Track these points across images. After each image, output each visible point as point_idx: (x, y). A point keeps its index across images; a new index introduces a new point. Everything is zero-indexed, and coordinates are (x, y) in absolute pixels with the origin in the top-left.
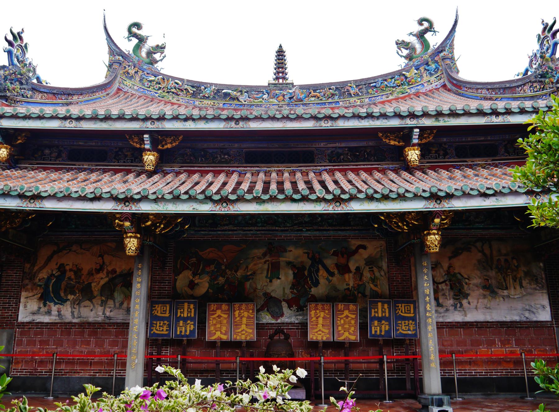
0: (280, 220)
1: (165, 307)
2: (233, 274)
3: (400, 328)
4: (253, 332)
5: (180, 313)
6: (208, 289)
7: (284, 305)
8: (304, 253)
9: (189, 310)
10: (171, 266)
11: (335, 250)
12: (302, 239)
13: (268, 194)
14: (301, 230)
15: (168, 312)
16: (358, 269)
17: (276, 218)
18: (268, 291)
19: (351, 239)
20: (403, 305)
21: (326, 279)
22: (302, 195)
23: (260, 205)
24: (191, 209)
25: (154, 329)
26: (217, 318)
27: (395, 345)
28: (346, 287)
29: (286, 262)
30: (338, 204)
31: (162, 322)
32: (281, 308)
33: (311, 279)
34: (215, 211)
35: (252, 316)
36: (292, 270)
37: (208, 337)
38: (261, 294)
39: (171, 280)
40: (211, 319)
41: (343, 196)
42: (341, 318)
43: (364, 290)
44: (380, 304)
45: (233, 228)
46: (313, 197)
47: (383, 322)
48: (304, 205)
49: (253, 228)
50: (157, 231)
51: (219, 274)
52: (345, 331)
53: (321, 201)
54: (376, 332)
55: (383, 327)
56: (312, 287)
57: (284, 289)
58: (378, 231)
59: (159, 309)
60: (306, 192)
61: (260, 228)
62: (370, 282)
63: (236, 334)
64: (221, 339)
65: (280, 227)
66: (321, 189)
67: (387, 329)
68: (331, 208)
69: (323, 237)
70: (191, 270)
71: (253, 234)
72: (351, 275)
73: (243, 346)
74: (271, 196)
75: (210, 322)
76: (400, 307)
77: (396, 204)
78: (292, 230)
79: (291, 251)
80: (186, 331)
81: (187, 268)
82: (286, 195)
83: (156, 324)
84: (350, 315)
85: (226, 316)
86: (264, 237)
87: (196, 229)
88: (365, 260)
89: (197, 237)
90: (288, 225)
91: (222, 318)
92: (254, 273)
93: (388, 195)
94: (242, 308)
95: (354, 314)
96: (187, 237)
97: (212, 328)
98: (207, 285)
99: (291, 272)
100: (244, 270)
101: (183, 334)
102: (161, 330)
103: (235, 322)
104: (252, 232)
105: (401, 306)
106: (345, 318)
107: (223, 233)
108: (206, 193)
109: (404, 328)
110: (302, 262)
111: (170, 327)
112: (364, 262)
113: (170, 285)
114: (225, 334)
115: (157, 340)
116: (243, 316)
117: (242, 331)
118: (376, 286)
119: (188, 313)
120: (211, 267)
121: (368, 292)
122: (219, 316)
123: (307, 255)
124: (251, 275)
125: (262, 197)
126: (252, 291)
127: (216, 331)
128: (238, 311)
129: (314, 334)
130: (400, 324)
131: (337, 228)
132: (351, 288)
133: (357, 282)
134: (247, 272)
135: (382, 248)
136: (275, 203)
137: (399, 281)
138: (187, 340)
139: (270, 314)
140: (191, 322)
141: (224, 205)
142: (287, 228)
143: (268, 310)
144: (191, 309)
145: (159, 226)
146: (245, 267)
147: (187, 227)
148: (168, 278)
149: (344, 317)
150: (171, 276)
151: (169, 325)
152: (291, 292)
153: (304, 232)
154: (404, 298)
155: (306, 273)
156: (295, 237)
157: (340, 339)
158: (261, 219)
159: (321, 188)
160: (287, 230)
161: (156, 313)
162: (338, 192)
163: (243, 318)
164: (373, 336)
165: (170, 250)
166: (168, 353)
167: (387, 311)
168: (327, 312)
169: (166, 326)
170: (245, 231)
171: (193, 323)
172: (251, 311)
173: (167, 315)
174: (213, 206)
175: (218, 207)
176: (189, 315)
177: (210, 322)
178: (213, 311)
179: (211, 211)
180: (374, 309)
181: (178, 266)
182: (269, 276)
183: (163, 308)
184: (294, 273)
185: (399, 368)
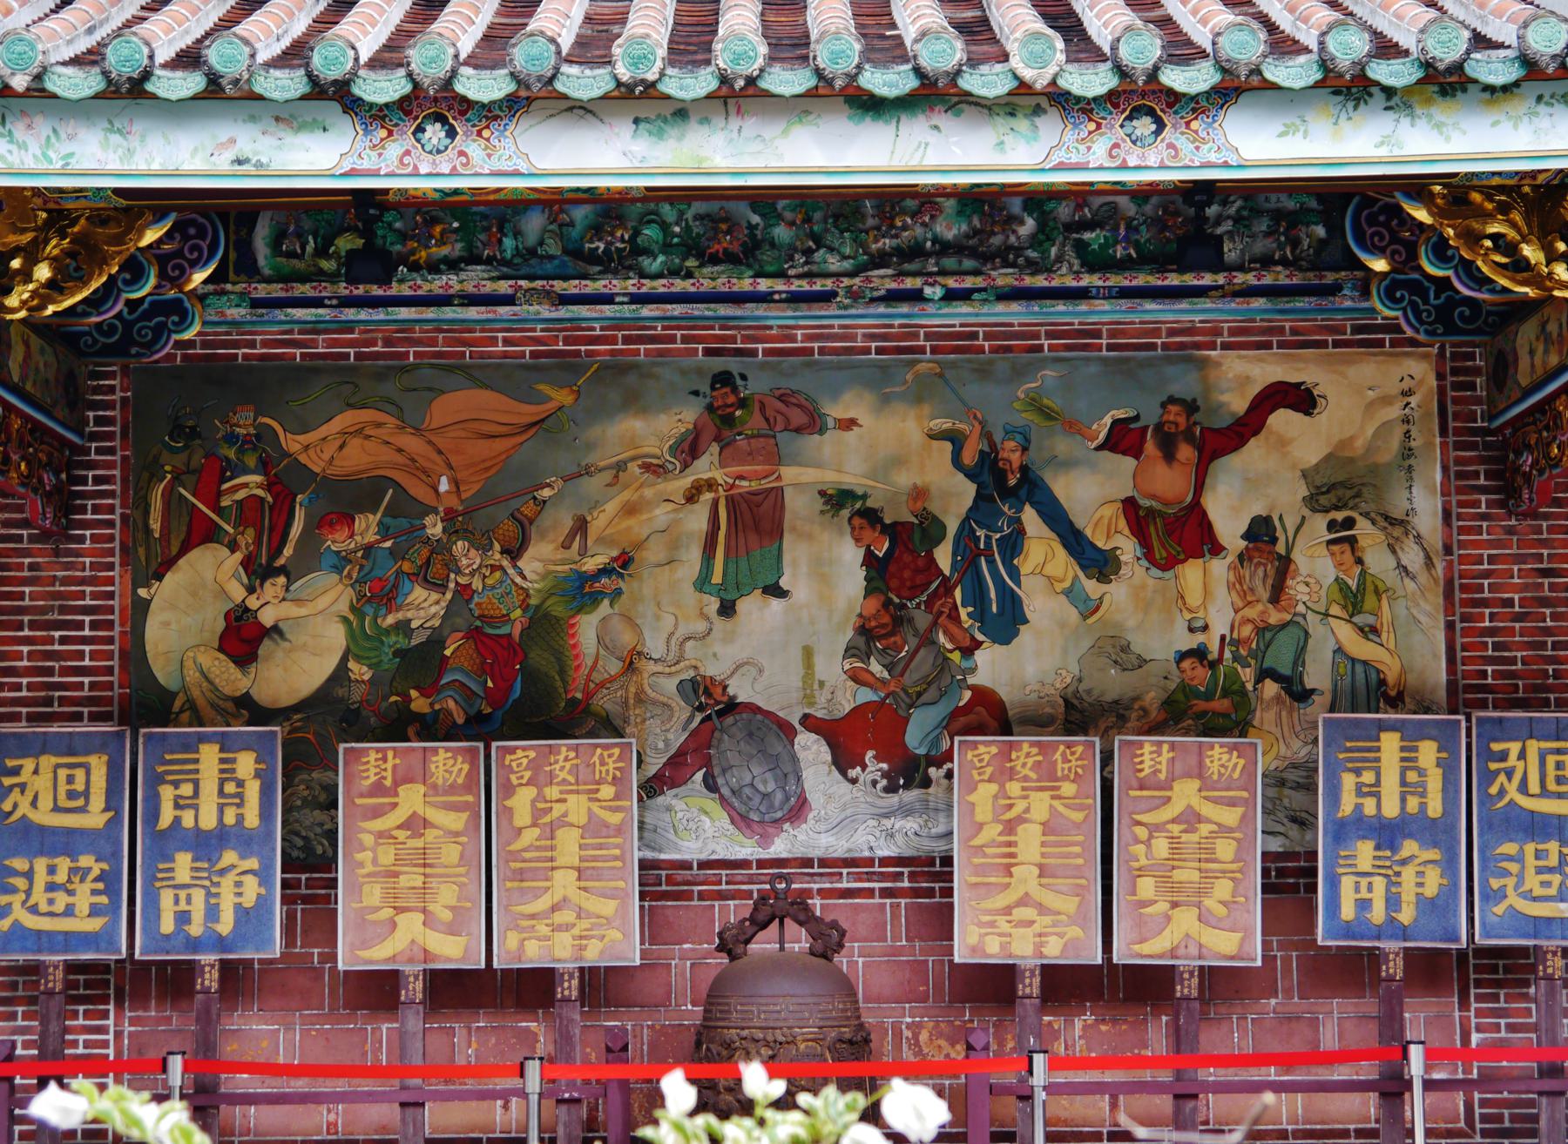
0: (781, 233)
1: (80, 774)
2: (494, 568)
3: (1510, 882)
4: (623, 911)
5: (177, 806)
6: (344, 659)
7: (812, 750)
8: (934, 436)
9: (230, 788)
10: (110, 524)
12: (922, 350)
13: (708, 62)
14: (916, 296)
15: (98, 801)
16: (1261, 532)
17: (756, 219)
18: (712, 670)
19: (1226, 346)
20: (1533, 746)
21: (1068, 593)
22: (917, 71)
23: (660, 134)
24: (223, 162)
25: (17, 906)
26: (402, 835)
27: (1478, 984)
28: (1189, 642)
29: (822, 493)
30: (1144, 126)
31: (64, 864)
32: (789, 771)
33: (977, 597)
34: (375, 174)
36: (857, 540)
37: (353, 948)
38: (671, 685)
39: (111, 610)
40: (368, 839)
41: (1174, 78)
42: (1154, 829)
44: (1390, 743)
45: (489, 287)
46: (988, 82)
47: (1409, 847)
48: (932, 137)
49: (617, 285)
50: (12, 301)
51: (406, 567)
52: (1175, 905)
53: (1038, 111)
54: (1364, 905)
55: (1408, 874)
56: (978, 644)
57: (808, 653)
58: (1390, 297)
59: (42, 783)
60: (944, 53)
61: (660, 286)
62: (1335, 610)
63: (517, 928)
64: (427, 955)
65: (781, 275)
66: (1037, 35)
67: (1431, 890)
68: (1099, 150)
69: (1050, 335)
70: (233, 547)
71: (617, 324)
72: (1219, 568)
74: (724, 79)
75: (359, 856)
76: (1512, 760)
77: (1506, 126)
78: (855, 296)
79: (848, 424)
80: (212, 913)
81: (202, 533)
82: (818, 72)
83: (29, 875)
84: (1207, 809)
85: (456, 821)
86: (685, 339)
87: (262, 291)
88: (1305, 475)
89: (265, 344)
90: (834, 264)
91: (431, 834)
92: (625, 561)
93: (1458, 68)
94: (551, 775)
95: (1232, 803)
96: (205, 345)
97: (373, 894)
98: (335, 638)
99: (849, 555)
100: (566, 546)
101: (196, 929)
102: (59, 907)
104: (608, 310)
105: (1522, 755)
106: (1176, 829)
107: (430, 313)
108: (317, 60)
109: (1532, 882)
110: (919, 493)
111: (111, 890)
112: (1303, 491)
113: (110, 641)
114: (452, 930)
115: (35, 969)
116: (562, 822)
117: (555, 908)
118: (1370, 632)
119: (221, 809)
120: (360, 523)
121: (1317, 675)
122: (416, 824)
123: (948, 446)
124: (605, 571)
125: (669, 87)
126: (614, 667)
127: (400, 910)
129: (992, 924)
130: (1510, 858)
131: (1142, 280)
132: (1214, 647)
133: (1251, 613)
134: (583, 552)
135: (1414, 400)
136: (751, 125)
137: (1509, 603)
138: (224, 964)
139: (723, 801)
140: (242, 857)
141: (434, 133)
142: (829, 284)
143: (711, 785)
144: (240, 784)
145: (26, 275)
146: (568, 523)
147: (199, 277)
148: (94, 596)
150: (110, 581)
151: (108, 881)
152: (855, 677)
153: (930, 308)
154: (1544, 705)
155: (944, 557)
156: (873, 337)
157: (1146, 948)
158: (664, 226)
159: (1040, 26)
160: (826, 297)
162: (1143, 50)
163: (559, 833)
164: (1348, 930)
165: (99, 421)
166: (105, 1044)
167: (1434, 782)
168: (1068, 789)
169: (88, 886)
170: (566, 300)
171: (253, 863)
172: (607, 791)
173: (95, 818)
174: (362, 142)
175: (394, 150)
176: (230, 818)
177: (359, 856)
178: (378, 789)
179: (352, 173)
180: (1358, 772)
181: (155, 525)
182: (717, 578)
184: (869, 560)
185: (1500, 1118)
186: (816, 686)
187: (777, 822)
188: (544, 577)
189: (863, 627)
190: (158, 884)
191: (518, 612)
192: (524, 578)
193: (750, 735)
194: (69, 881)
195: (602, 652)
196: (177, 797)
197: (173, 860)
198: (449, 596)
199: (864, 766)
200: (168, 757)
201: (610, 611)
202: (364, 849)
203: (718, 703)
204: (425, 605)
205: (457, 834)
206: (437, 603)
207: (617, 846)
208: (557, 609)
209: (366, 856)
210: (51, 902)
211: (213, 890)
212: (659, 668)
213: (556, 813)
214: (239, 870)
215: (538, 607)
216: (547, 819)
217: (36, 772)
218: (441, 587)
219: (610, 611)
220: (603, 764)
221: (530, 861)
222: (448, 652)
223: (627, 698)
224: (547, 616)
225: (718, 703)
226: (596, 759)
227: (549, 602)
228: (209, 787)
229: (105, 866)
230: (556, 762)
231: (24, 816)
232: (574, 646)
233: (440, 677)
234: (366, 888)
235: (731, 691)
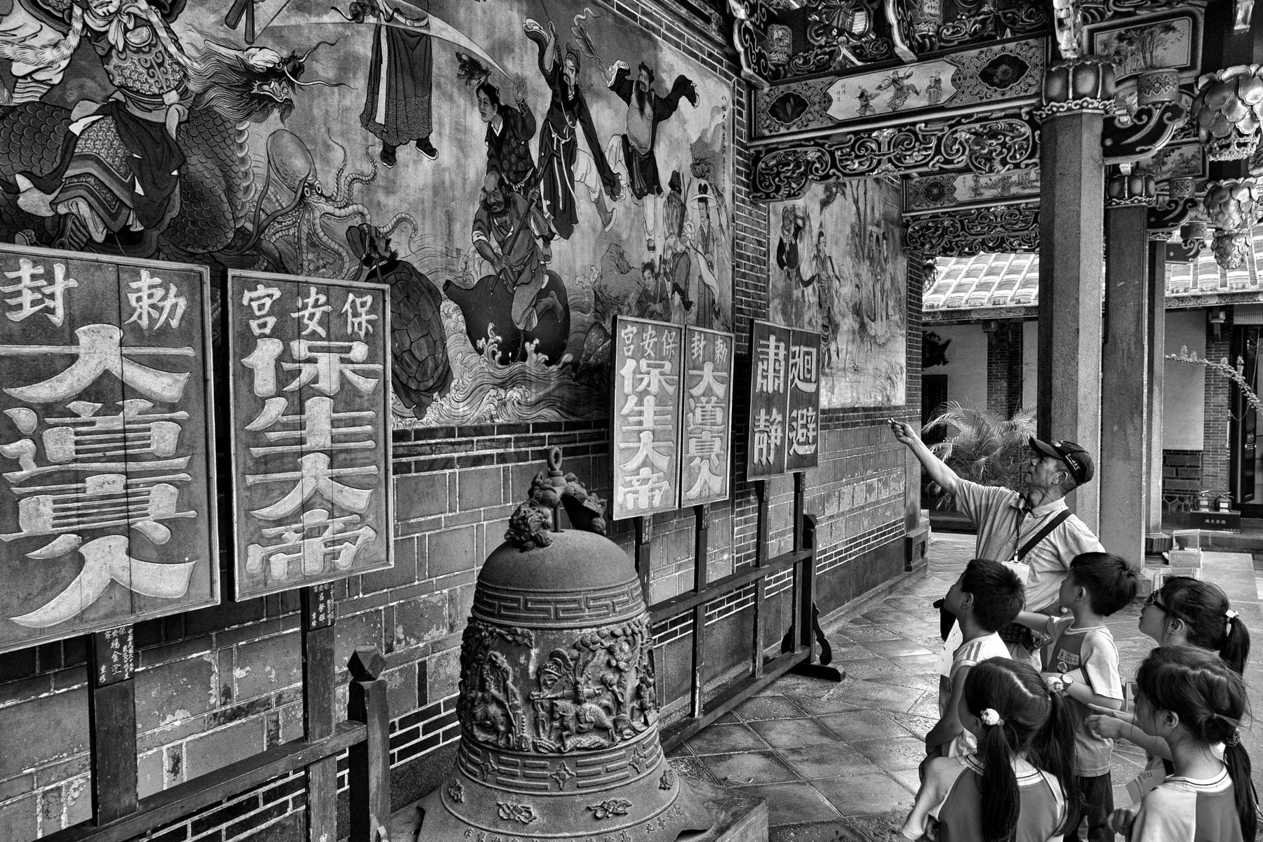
2: (141, 22)
11: (619, 64)
35: (366, 385)
38: (341, 230)
43: (687, 284)
72: (661, 201)
103: (257, 438)
124: (272, 73)
149: (703, 395)
182: (380, 118)
186: (454, 254)
187: (430, 390)
188: (207, 55)
189: (485, 200)
191: (172, 97)
192: (180, 49)
193: (408, 297)
195: (273, 175)
198: (73, 40)
199: (487, 339)
201: (281, 126)
202: (18, 435)
203: (382, 258)
204: (34, 42)
206: (56, 46)
208: (224, 106)
212: (329, 208)
215: (199, 95)
218: (62, 22)
219: (281, 126)
221: (276, 444)
222: (76, 129)
223: (299, 239)
224: (209, 110)
225: (382, 258)
227: (212, 94)
232: (243, 161)
233: (64, 166)
235: (393, 247)
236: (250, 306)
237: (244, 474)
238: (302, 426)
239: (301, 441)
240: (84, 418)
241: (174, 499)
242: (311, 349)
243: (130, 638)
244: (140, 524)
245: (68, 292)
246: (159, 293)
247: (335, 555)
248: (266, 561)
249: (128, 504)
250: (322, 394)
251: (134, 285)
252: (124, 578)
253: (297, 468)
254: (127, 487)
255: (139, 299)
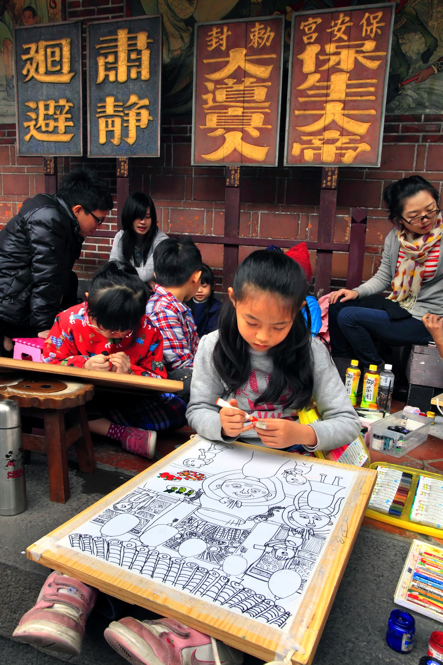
5: (107, 69)
15: (66, 68)
35: (373, 65)
59: (40, 57)
73: (328, 189)
75: (204, 97)
83: (36, 110)
94: (332, 34)
102: (51, 129)
103: (303, 93)
116: (336, 69)
117: (326, 129)
119: (129, 68)
128: (316, 49)
140: (140, 98)
144: (139, 52)
161: (32, 73)
163: (334, 78)
171: (146, 102)
172: (369, 45)
183: (53, 54)
190: (98, 116)
194: (55, 113)
196: (107, 63)
197: (105, 102)
200: (101, 39)
205: (264, 80)
207: (372, 85)
209: (209, 97)
210: (47, 125)
211: (126, 118)
213: (332, 63)
214: (138, 106)
216: (326, 67)
217: (37, 51)
220: (369, 24)
226: (364, 21)
228: (122, 56)
229: (71, 105)
230: (336, 25)
231: (33, 77)
234: (208, 117)
236: (304, 30)
237: (294, 110)
238: (328, 88)
239: (327, 95)
240: (230, 85)
241: (262, 120)
242: (337, 47)
243: (238, 171)
244: (247, 128)
245: (228, 37)
246: (263, 31)
247: (342, 155)
248: (302, 151)
249: (243, 120)
250: (342, 71)
251: (253, 30)
252: (239, 149)
253: (323, 109)
254: (243, 113)
255: (254, 36)
